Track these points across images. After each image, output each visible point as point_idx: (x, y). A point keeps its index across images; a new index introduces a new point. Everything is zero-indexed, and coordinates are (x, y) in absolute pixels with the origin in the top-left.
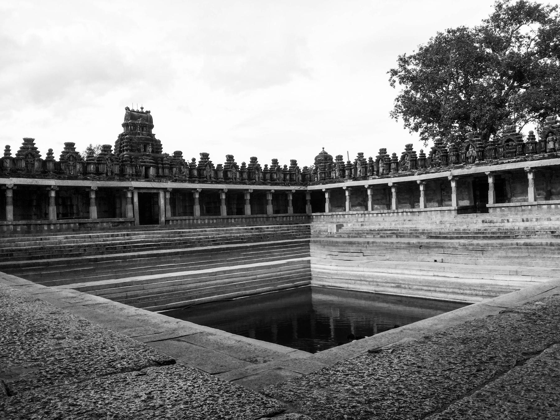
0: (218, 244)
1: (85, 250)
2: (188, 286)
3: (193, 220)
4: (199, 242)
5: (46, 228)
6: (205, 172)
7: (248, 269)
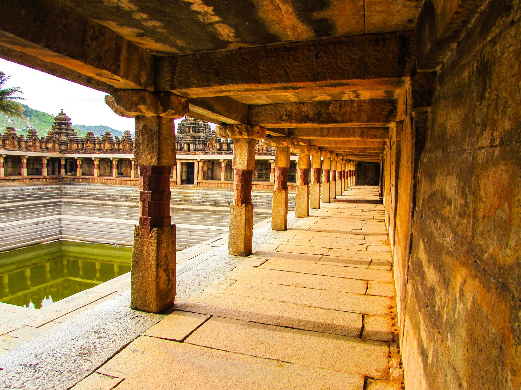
0: (203, 205)
2: (111, 230)
4: (191, 201)
5: (129, 182)
6: (232, 145)
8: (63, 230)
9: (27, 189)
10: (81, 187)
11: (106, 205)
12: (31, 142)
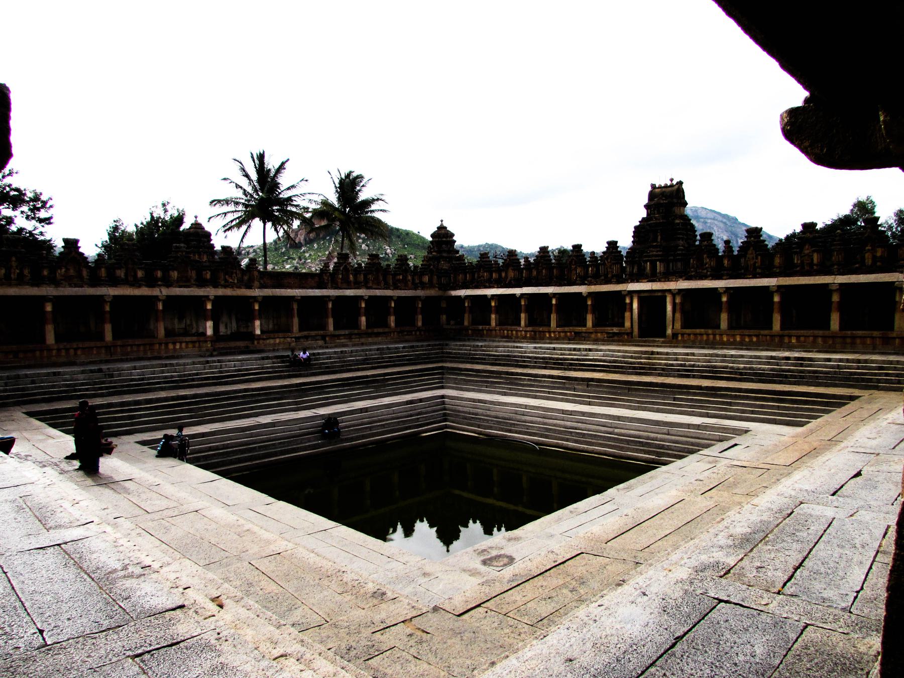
1: (536, 362)
3: (714, 335)
4: (663, 369)
7: (619, 418)
8: (449, 415)
9: (396, 348)
10: (472, 344)
11: (512, 374)
12: (400, 274)
